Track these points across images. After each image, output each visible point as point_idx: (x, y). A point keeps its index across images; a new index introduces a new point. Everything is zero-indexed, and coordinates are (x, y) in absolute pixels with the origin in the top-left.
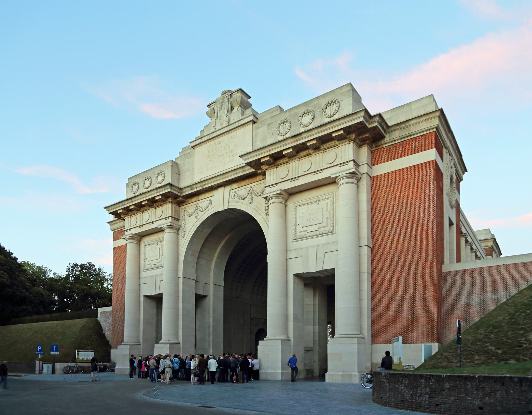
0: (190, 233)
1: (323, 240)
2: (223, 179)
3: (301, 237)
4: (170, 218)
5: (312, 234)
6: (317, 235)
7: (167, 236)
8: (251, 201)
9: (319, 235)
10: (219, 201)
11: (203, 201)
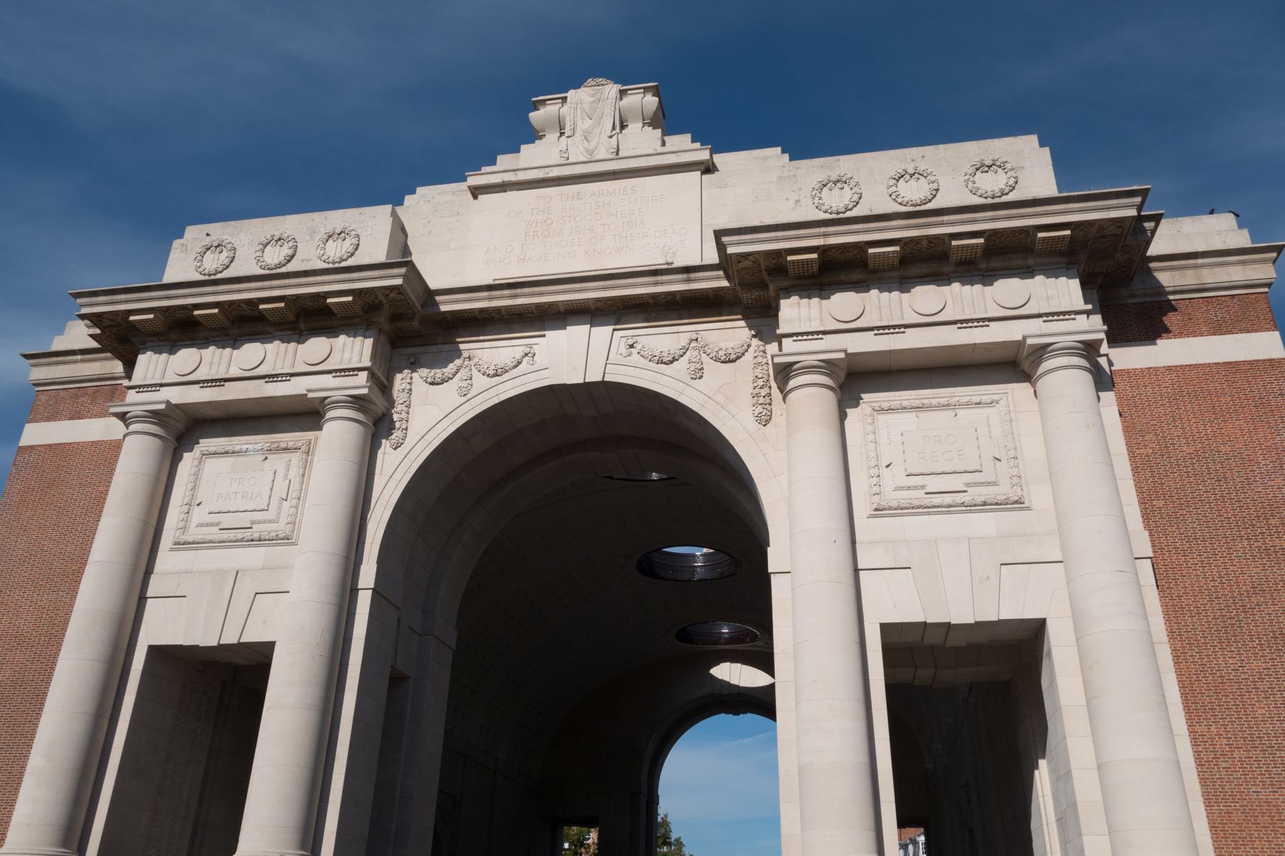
0: (429, 438)
1: (984, 523)
2: (604, 288)
3: (894, 504)
4: (364, 375)
5: (947, 499)
6: (963, 504)
7: (338, 435)
8: (698, 374)
9: (971, 507)
10: (570, 357)
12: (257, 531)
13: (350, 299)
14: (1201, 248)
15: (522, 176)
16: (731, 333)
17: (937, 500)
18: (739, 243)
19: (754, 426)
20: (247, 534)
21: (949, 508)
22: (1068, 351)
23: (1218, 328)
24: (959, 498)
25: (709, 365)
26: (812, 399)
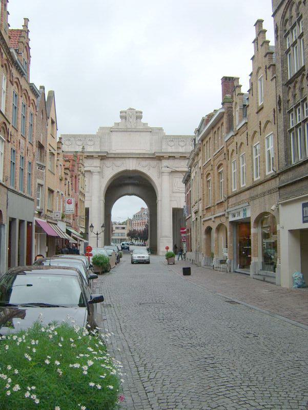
11: (118, 162)
15: (120, 130)
16: (154, 163)
26: (166, 178)
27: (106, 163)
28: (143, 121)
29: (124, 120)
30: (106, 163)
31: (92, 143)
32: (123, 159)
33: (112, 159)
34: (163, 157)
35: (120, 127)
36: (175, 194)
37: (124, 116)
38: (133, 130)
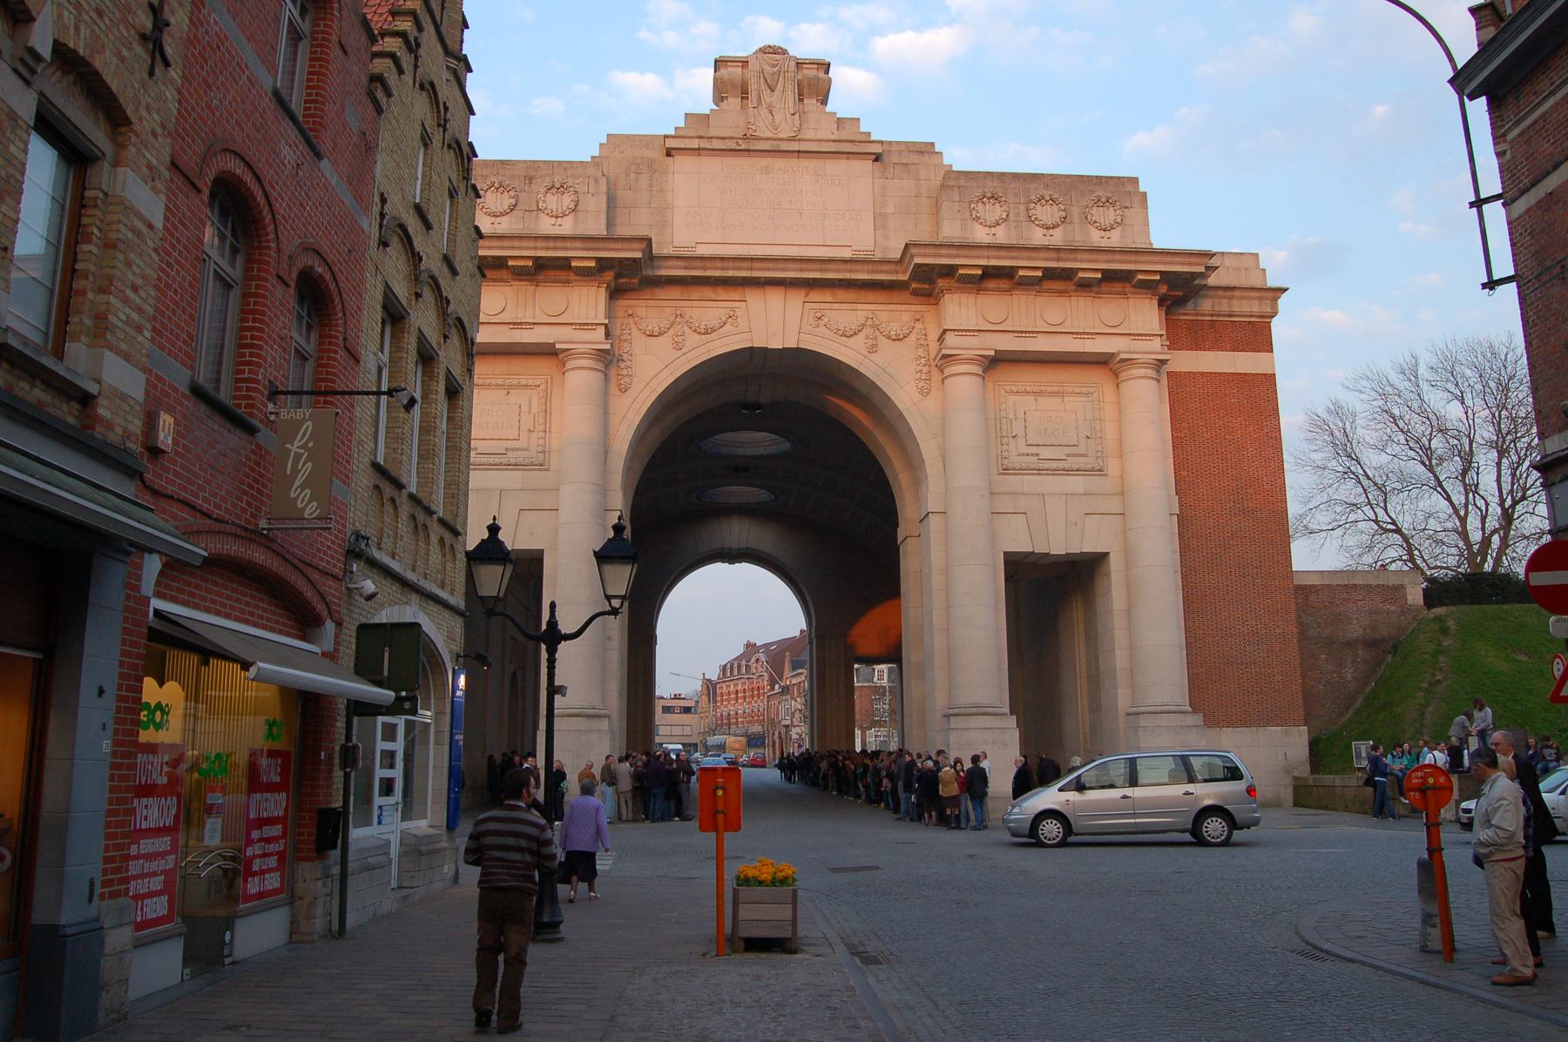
1: (1076, 484)
5: (1054, 465)
7: (581, 380)
8: (873, 349)
9: (1067, 472)
11: (707, 310)
12: (512, 457)
13: (593, 264)
14: (1234, 283)
15: (717, 144)
17: (1047, 465)
18: (924, 256)
19: (917, 397)
20: (504, 460)
21: (1055, 472)
22: (1145, 365)
23: (1237, 347)
24: (1061, 465)
25: (883, 341)
26: (964, 385)
27: (642, 312)
28: (838, 104)
29: (734, 102)
30: (642, 312)
31: (567, 201)
32: (735, 295)
33: (674, 292)
34: (949, 271)
35: (713, 132)
36: (1012, 482)
37: (733, 81)
38: (785, 146)
